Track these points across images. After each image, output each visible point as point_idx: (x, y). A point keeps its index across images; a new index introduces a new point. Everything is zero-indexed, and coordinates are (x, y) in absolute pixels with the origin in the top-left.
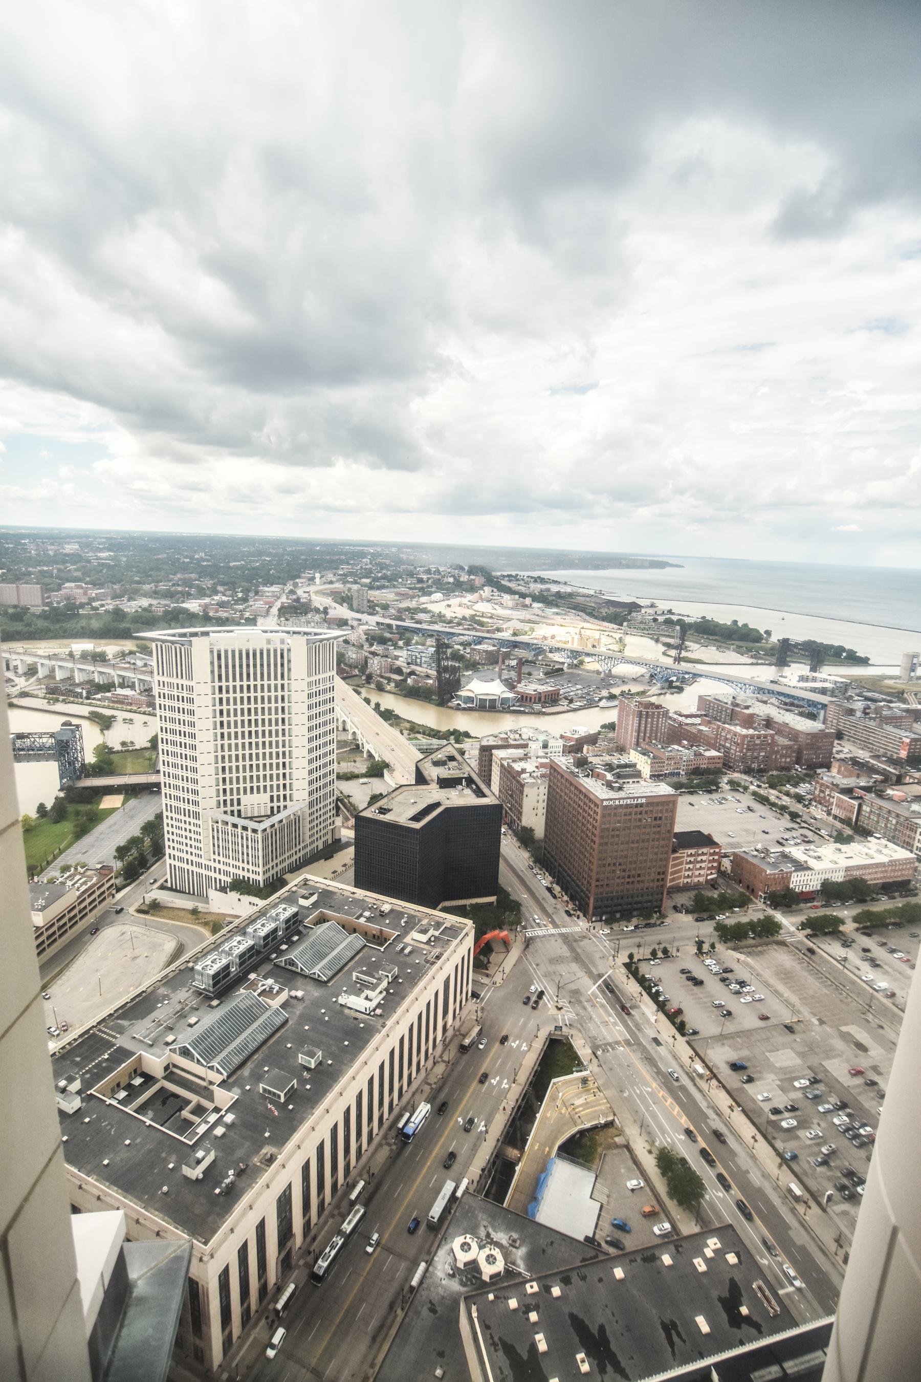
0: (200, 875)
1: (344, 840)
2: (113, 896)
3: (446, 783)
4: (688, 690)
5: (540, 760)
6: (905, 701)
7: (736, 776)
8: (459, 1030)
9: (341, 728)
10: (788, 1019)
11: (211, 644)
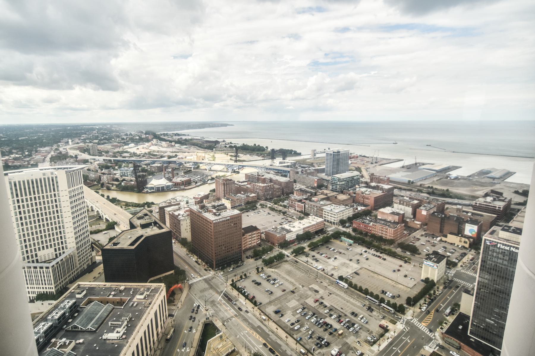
1: (98, 262)
3: (144, 226)
6: (314, 166)
7: (262, 202)
8: (164, 333)
9: (90, 210)
10: (292, 288)
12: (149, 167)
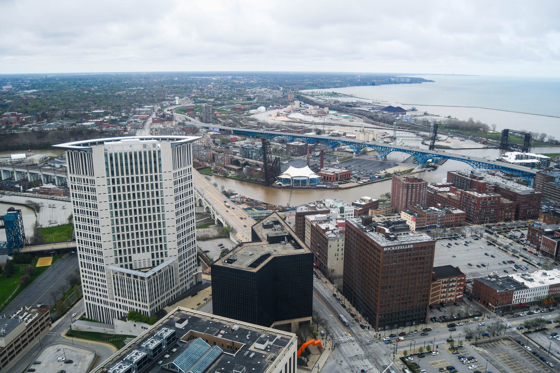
0: (107, 310)
1: (204, 282)
2: (50, 325)
4: (440, 168)
5: (339, 221)
9: (198, 205)
11: (105, 150)
12: (285, 146)
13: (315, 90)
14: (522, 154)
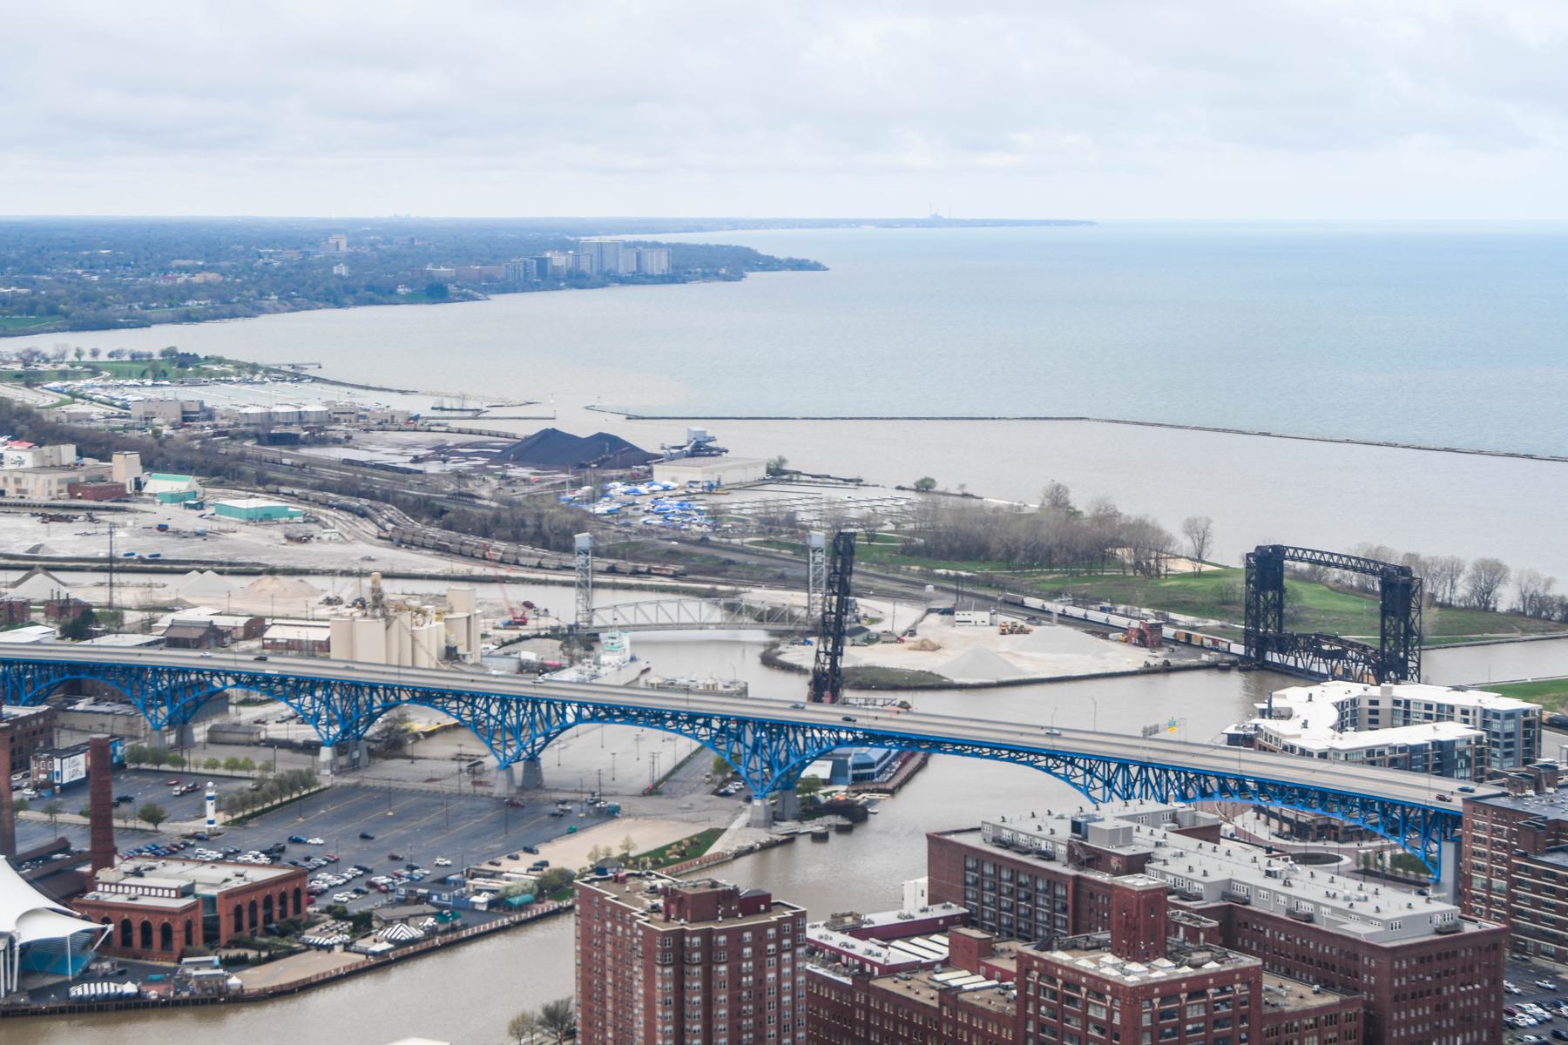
13: (47, 343)
14: (1375, 691)
